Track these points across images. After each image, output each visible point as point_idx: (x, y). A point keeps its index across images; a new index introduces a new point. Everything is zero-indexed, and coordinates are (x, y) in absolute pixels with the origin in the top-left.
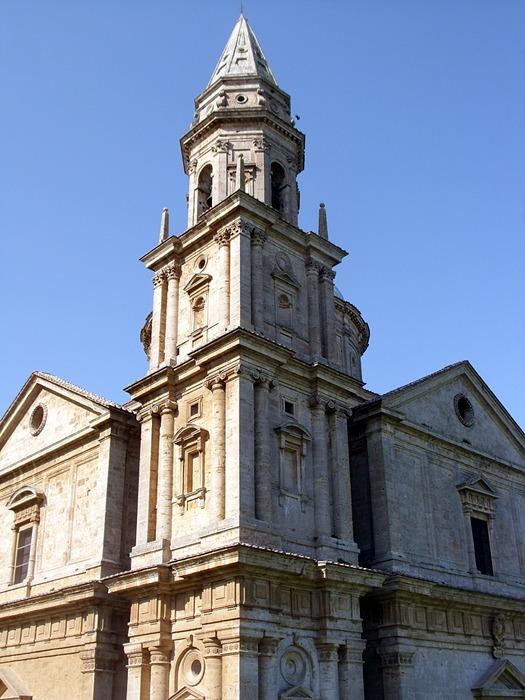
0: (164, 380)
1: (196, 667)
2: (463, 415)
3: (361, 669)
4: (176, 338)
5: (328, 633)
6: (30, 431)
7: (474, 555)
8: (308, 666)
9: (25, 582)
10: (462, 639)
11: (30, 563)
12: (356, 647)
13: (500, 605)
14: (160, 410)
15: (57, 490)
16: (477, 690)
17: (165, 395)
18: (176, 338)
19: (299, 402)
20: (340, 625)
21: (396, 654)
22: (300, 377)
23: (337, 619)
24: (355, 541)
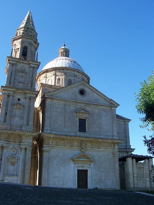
10: (69, 147)
19: (22, 98)
20: (25, 143)
21: (43, 150)
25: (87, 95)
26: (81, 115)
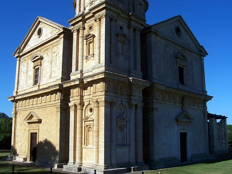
0: (80, 18)
1: (91, 110)
2: (178, 33)
3: (142, 111)
4: (84, 5)
5: (132, 100)
6: (37, 36)
7: (178, 78)
8: (126, 110)
9: (38, 84)
10: (173, 104)
11: (39, 79)
12: (141, 105)
13: (186, 94)
14: (79, 28)
15: (46, 55)
16: (177, 119)
17: (81, 23)
18: (84, 5)
20: (136, 98)
23: (135, 96)
24: (141, 72)
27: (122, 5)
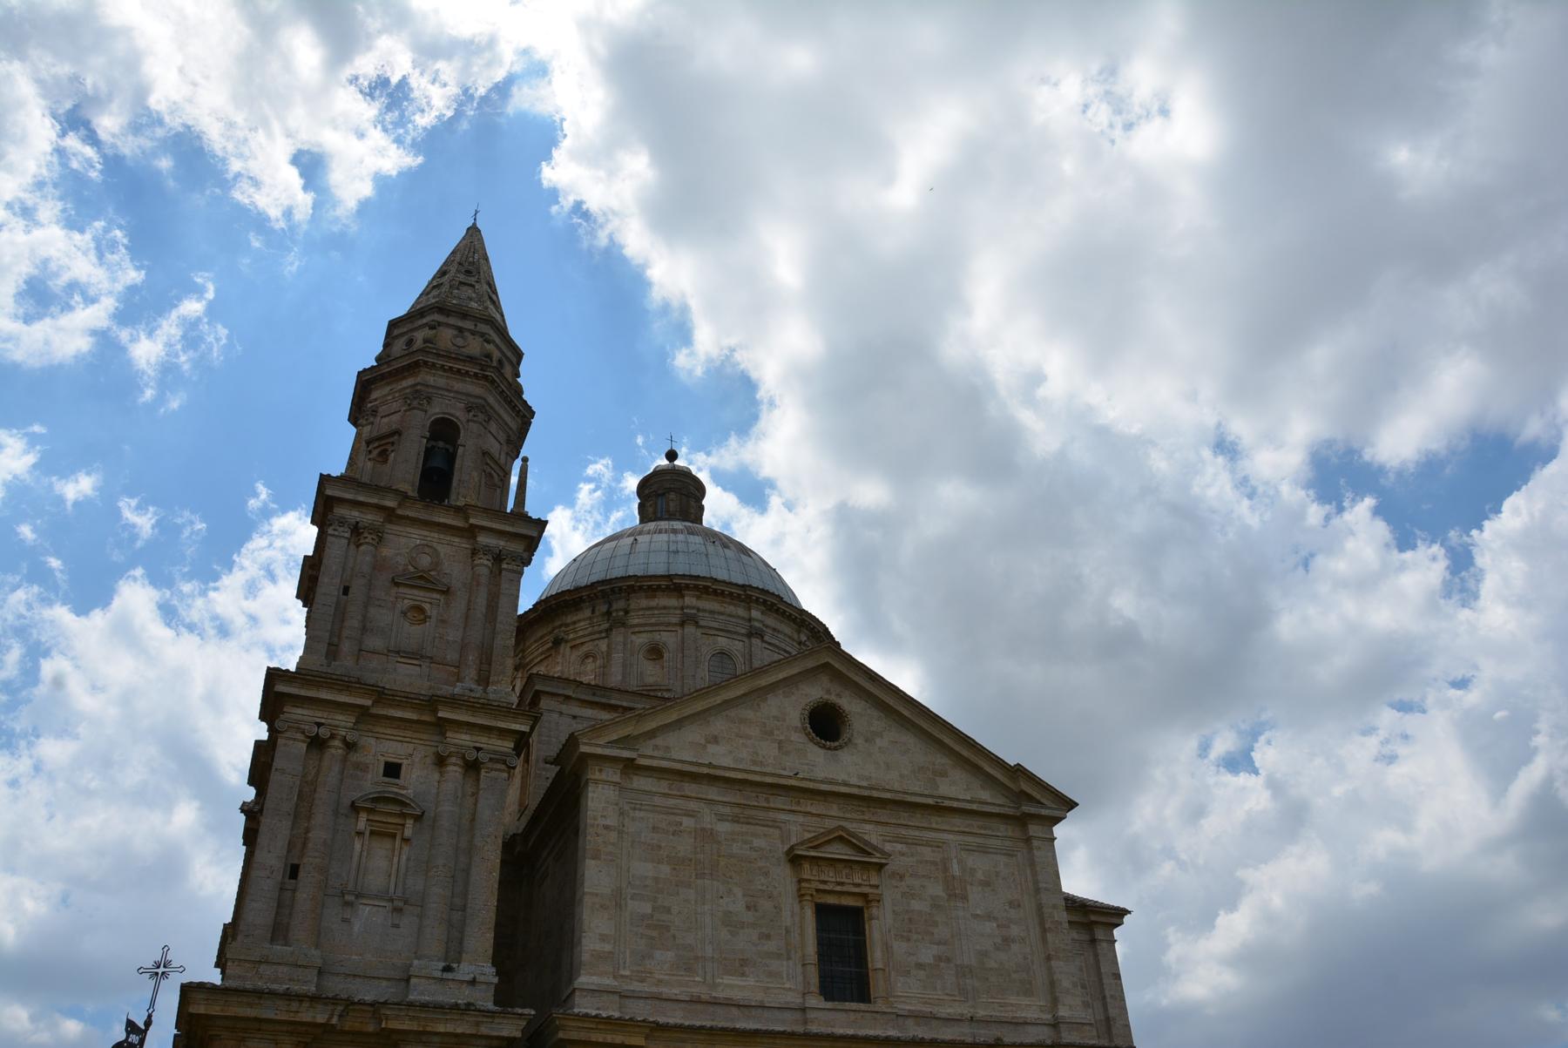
22: (418, 722)
24: (494, 964)
25: (859, 741)
26: (829, 875)
27: (418, 668)
